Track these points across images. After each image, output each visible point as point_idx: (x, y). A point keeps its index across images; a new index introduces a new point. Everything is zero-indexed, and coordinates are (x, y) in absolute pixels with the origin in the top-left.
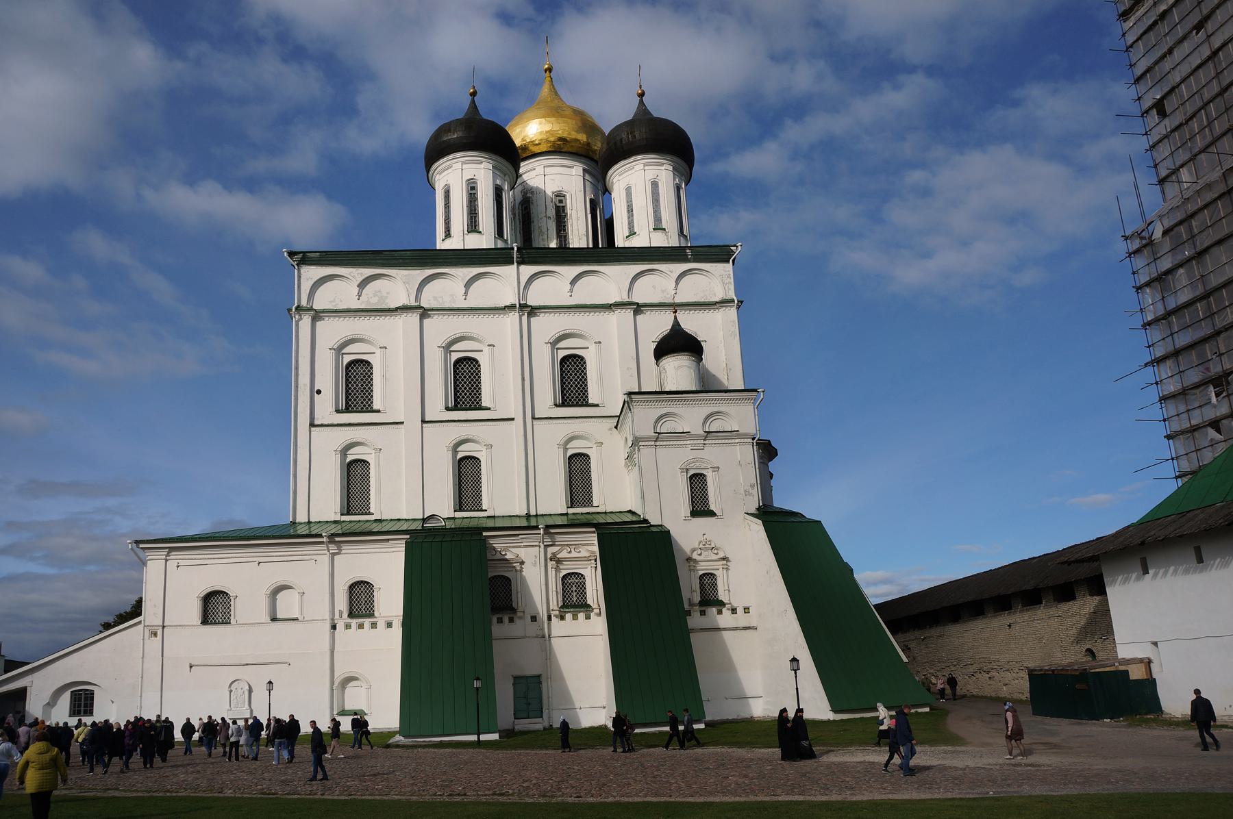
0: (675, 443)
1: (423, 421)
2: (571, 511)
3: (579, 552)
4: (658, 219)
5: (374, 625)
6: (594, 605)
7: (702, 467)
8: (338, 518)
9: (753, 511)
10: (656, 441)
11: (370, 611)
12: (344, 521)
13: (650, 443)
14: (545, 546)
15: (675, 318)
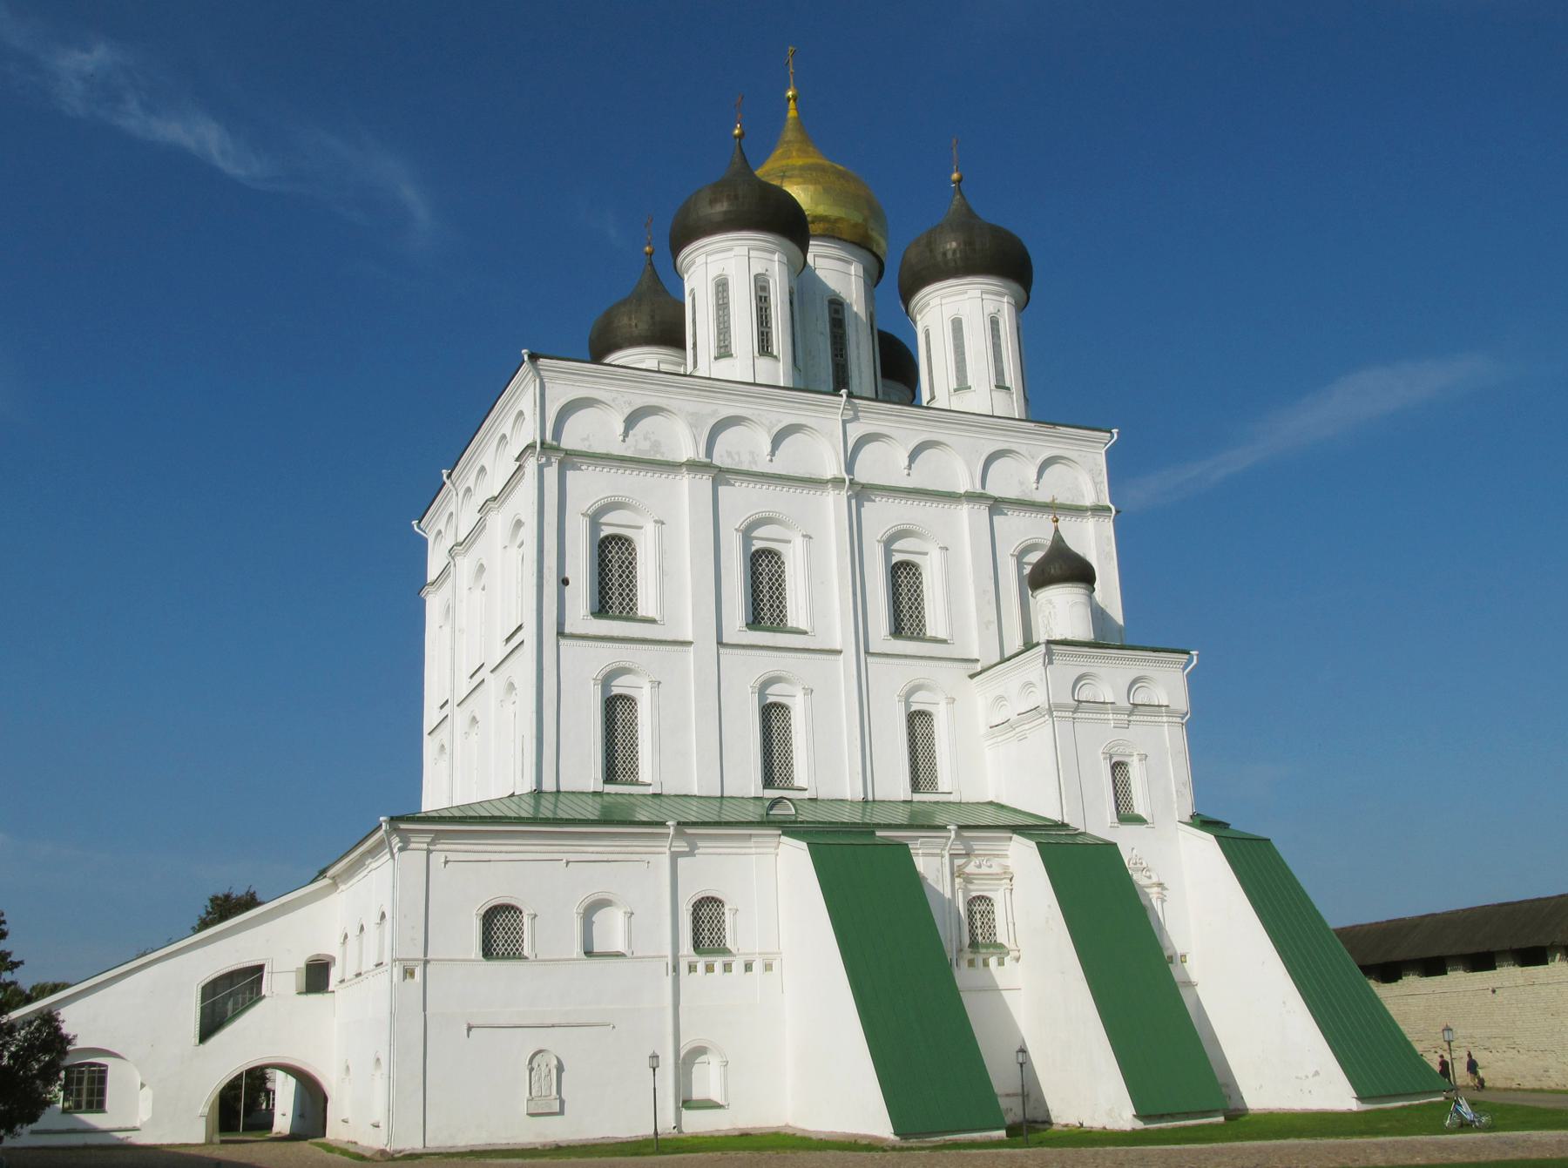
0: (1095, 716)
1: (720, 643)
2: (917, 797)
3: (990, 866)
4: (999, 373)
5: (727, 967)
6: (1009, 945)
7: (1127, 753)
8: (600, 787)
9: (1187, 819)
10: (1074, 712)
11: (719, 945)
12: (608, 794)
13: (1067, 714)
14: (950, 855)
15: (1057, 530)
